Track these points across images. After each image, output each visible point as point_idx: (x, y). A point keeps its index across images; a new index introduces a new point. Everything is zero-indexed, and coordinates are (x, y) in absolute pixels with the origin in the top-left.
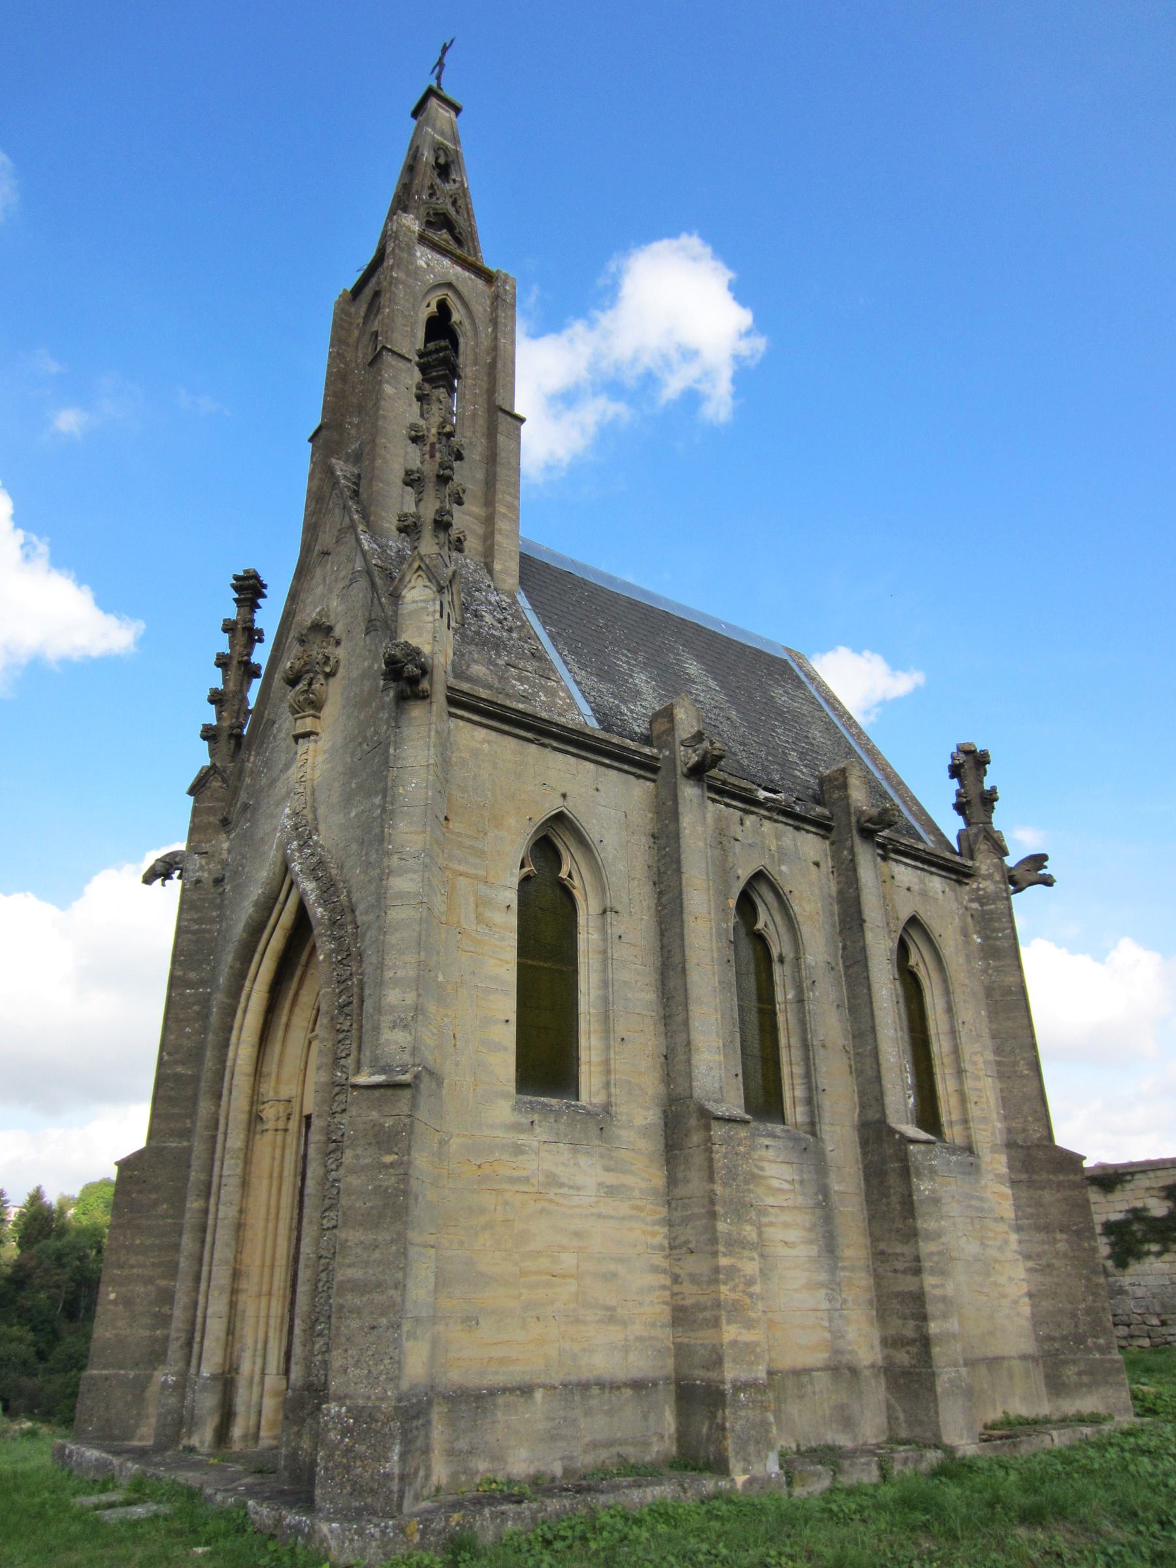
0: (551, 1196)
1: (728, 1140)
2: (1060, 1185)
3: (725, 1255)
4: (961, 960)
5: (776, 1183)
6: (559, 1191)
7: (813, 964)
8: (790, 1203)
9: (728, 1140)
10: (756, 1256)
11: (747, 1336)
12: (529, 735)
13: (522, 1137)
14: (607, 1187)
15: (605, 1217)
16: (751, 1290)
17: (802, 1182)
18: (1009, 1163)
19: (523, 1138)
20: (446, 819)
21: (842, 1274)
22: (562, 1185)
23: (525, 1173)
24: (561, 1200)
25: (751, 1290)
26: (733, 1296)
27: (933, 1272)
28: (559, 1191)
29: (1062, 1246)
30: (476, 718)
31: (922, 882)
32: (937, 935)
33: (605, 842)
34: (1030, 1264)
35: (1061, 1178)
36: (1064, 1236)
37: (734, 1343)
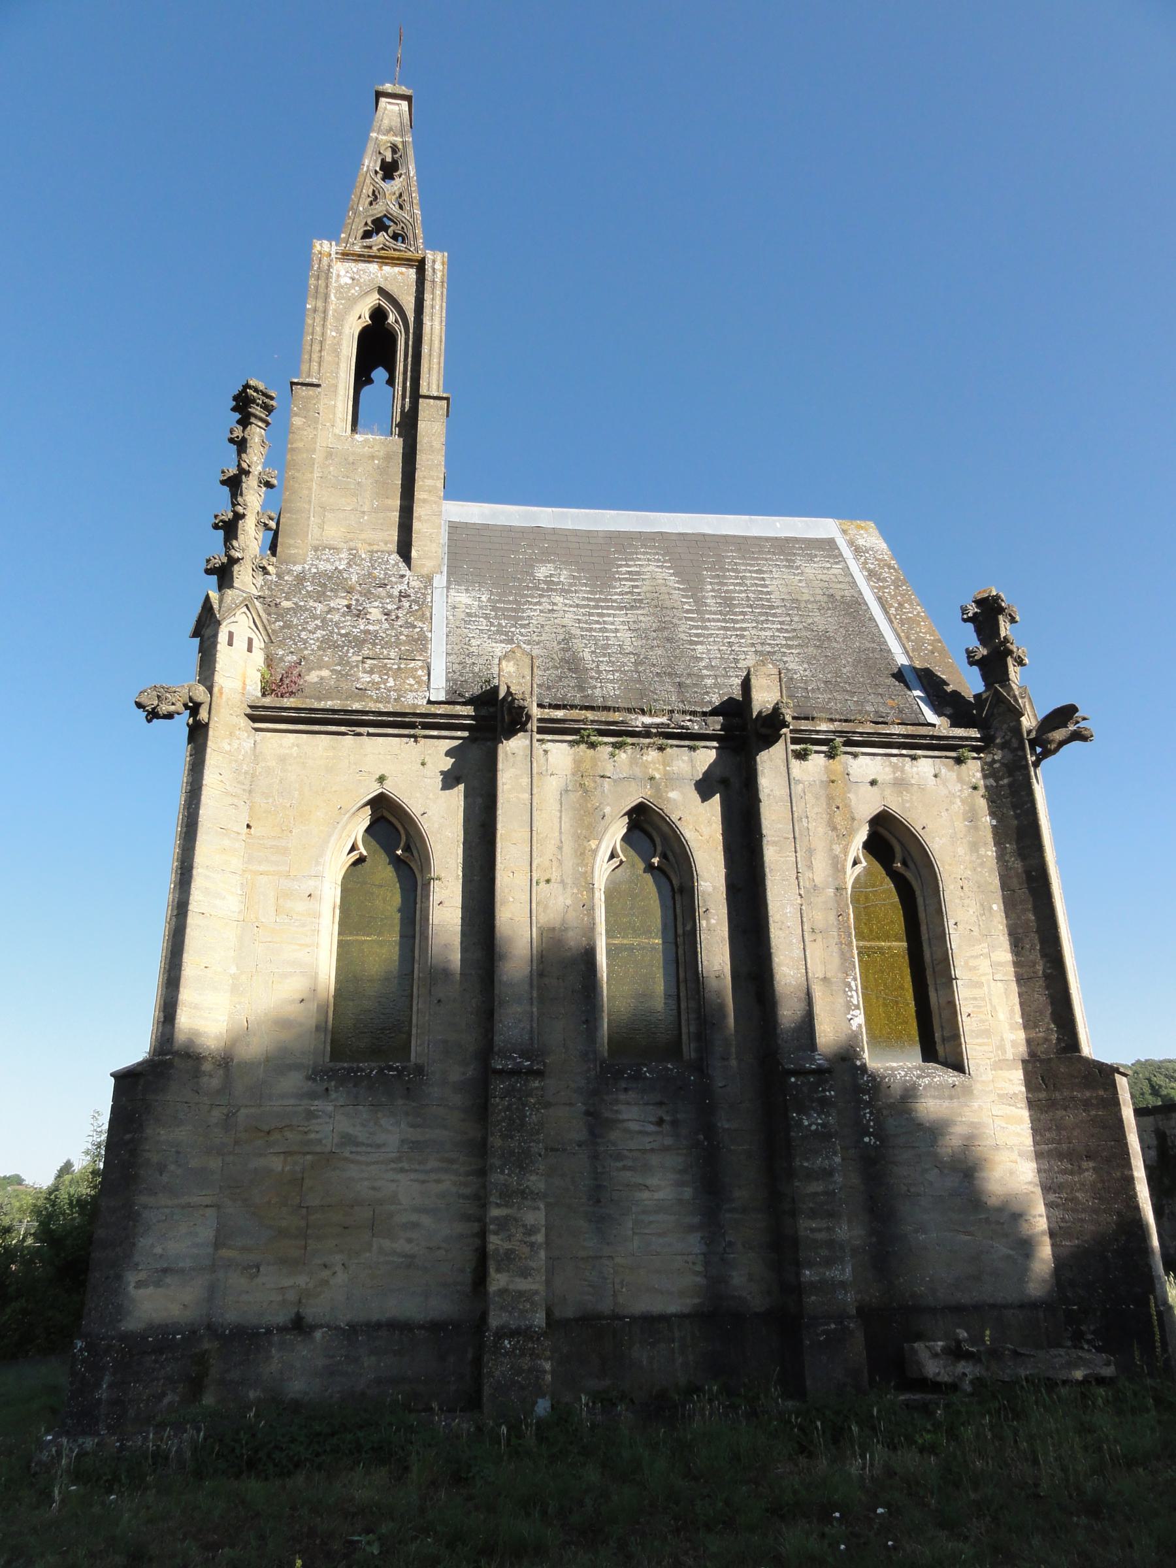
0: (347, 1154)
1: (508, 1093)
2: (1087, 1104)
3: (498, 1206)
4: (962, 850)
5: (634, 1126)
6: (354, 1149)
7: (710, 889)
8: (655, 1145)
9: (508, 1093)
10: (542, 1206)
11: (522, 1285)
12: (343, 729)
13: (316, 1103)
14: (413, 1142)
15: (407, 1171)
16: (533, 1239)
17: (675, 1123)
18: (1026, 1079)
19: (317, 1105)
20: (248, 826)
21: (728, 1215)
22: (357, 1144)
23: (318, 1136)
24: (358, 1158)
25: (533, 1239)
26: (507, 1245)
27: (813, 1214)
28: (354, 1149)
29: (1089, 1176)
30: (435, 733)
31: (895, 768)
32: (919, 828)
33: (429, 813)
34: (1052, 1197)
35: (1088, 1094)
36: (1091, 1164)
37: (503, 1292)
